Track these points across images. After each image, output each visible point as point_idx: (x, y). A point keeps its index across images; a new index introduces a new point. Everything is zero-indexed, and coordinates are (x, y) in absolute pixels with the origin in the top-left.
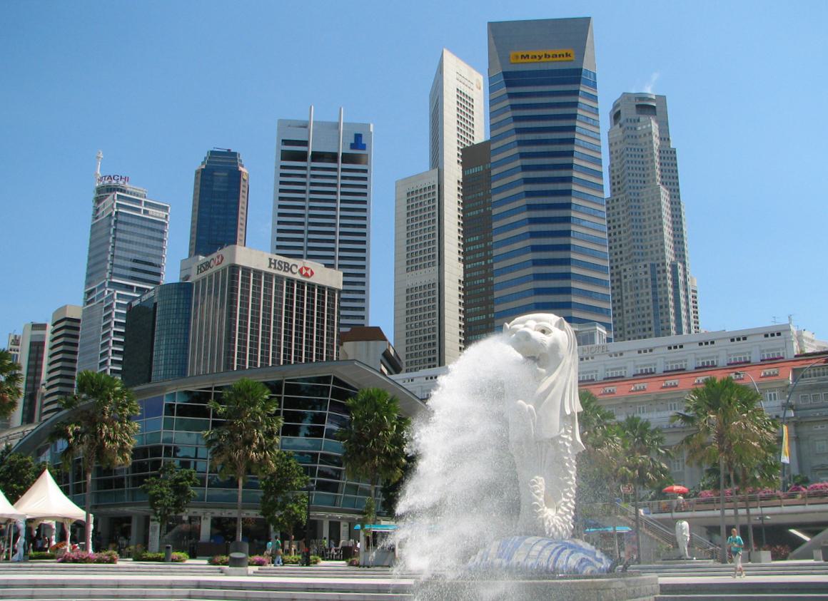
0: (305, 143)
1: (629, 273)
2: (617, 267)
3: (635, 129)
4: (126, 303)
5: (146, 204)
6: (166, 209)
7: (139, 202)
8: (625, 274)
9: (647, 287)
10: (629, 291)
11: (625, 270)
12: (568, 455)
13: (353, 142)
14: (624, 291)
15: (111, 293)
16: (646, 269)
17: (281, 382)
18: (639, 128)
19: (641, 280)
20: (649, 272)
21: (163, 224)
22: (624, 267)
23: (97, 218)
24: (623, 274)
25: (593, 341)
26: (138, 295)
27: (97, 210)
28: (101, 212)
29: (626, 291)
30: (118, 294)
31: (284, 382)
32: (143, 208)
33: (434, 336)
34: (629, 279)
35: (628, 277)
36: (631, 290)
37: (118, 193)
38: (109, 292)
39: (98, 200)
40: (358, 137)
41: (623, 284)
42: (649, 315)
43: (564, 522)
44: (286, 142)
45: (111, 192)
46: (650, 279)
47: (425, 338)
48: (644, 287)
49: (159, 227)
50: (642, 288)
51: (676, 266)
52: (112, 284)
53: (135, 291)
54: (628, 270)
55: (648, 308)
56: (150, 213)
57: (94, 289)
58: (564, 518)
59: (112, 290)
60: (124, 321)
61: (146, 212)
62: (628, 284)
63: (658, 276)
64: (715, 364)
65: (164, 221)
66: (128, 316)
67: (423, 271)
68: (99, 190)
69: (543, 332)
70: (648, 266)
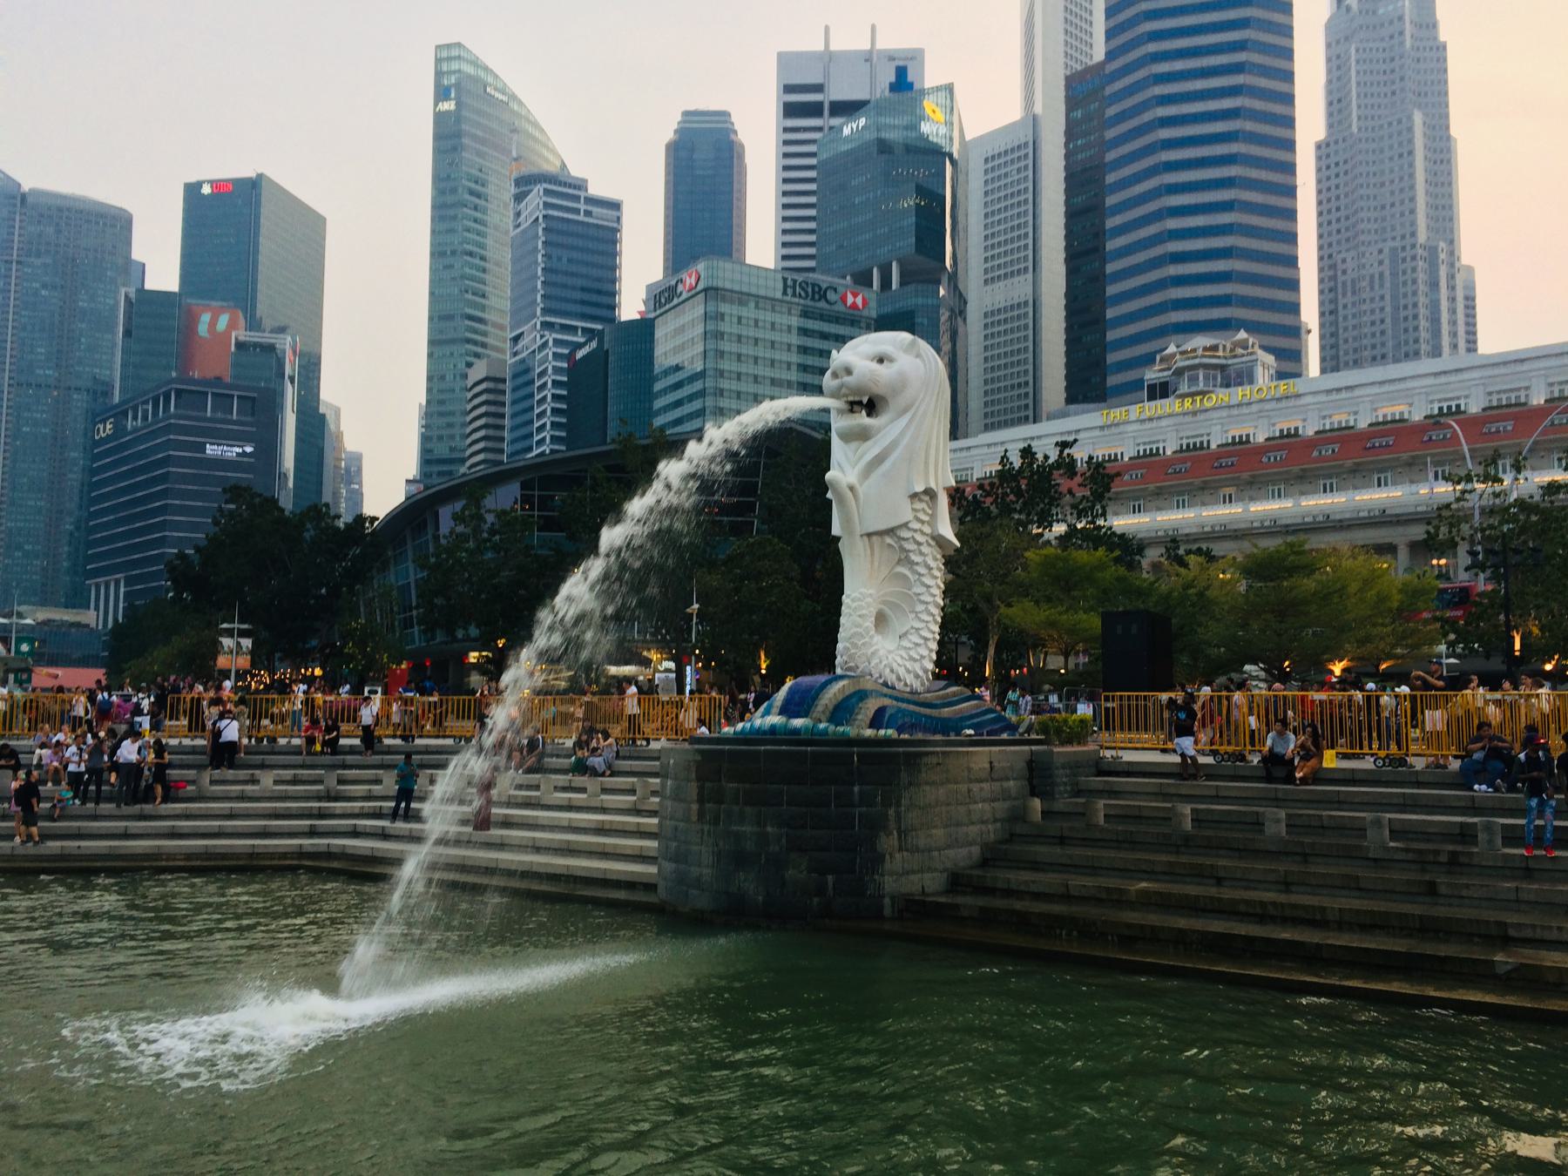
0: (818, 88)
1: (1350, 265)
2: (1330, 256)
3: (1374, 12)
4: (566, 351)
6: (615, 206)
7: (576, 198)
8: (1344, 267)
9: (1382, 286)
10: (1349, 294)
11: (1344, 261)
12: (921, 553)
13: (893, 79)
14: (1340, 297)
16: (1381, 257)
18: (1381, 11)
19: (1372, 276)
20: (1387, 262)
22: (1341, 256)
23: (519, 225)
24: (1340, 267)
25: (1251, 381)
26: (582, 340)
27: (518, 214)
28: (523, 216)
29: (1344, 295)
30: (554, 340)
32: (582, 207)
33: (1027, 383)
34: (1350, 275)
35: (1349, 272)
36: (1354, 293)
38: (542, 337)
39: (519, 198)
40: (901, 72)
41: (1340, 285)
42: (1383, 333)
43: (912, 659)
44: (789, 89)
45: (535, 184)
46: (1387, 273)
47: (1013, 387)
48: (1377, 287)
50: (1372, 288)
51: (1436, 248)
52: (546, 325)
54: (1349, 260)
55: (1382, 321)
57: (522, 334)
58: (913, 653)
59: (546, 333)
60: (565, 379)
61: (588, 213)
62: (1349, 284)
63: (1402, 267)
64: (1463, 408)
65: (615, 225)
66: (569, 372)
67: (1009, 281)
68: (518, 182)
69: (881, 361)
70: (1386, 251)
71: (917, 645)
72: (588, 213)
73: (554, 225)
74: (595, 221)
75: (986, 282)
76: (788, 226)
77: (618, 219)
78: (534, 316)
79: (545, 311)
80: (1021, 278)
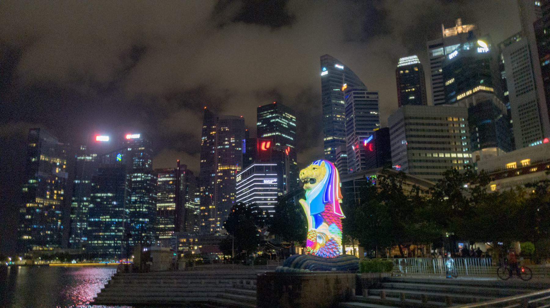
5: (367, 93)
6: (376, 93)
7: (364, 93)
15: (356, 138)
17: (353, 180)
21: (377, 101)
30: (360, 138)
31: (354, 181)
32: (366, 95)
37: (353, 91)
43: (328, 249)
49: (374, 103)
53: (368, 134)
56: (370, 97)
58: (329, 247)
61: (368, 97)
71: (330, 244)
72: (368, 97)
73: (357, 103)
74: (370, 99)
75: (517, 96)
76: (435, 90)
77: (378, 97)
78: (353, 131)
79: (357, 129)
80: (530, 93)
